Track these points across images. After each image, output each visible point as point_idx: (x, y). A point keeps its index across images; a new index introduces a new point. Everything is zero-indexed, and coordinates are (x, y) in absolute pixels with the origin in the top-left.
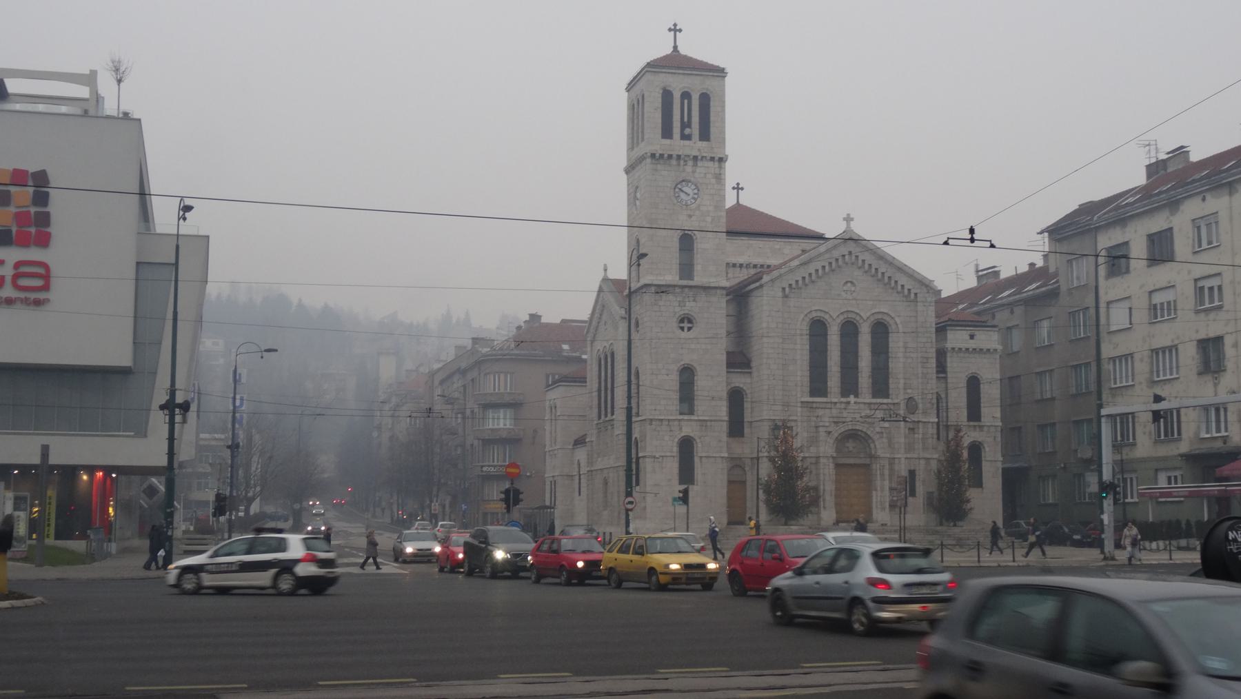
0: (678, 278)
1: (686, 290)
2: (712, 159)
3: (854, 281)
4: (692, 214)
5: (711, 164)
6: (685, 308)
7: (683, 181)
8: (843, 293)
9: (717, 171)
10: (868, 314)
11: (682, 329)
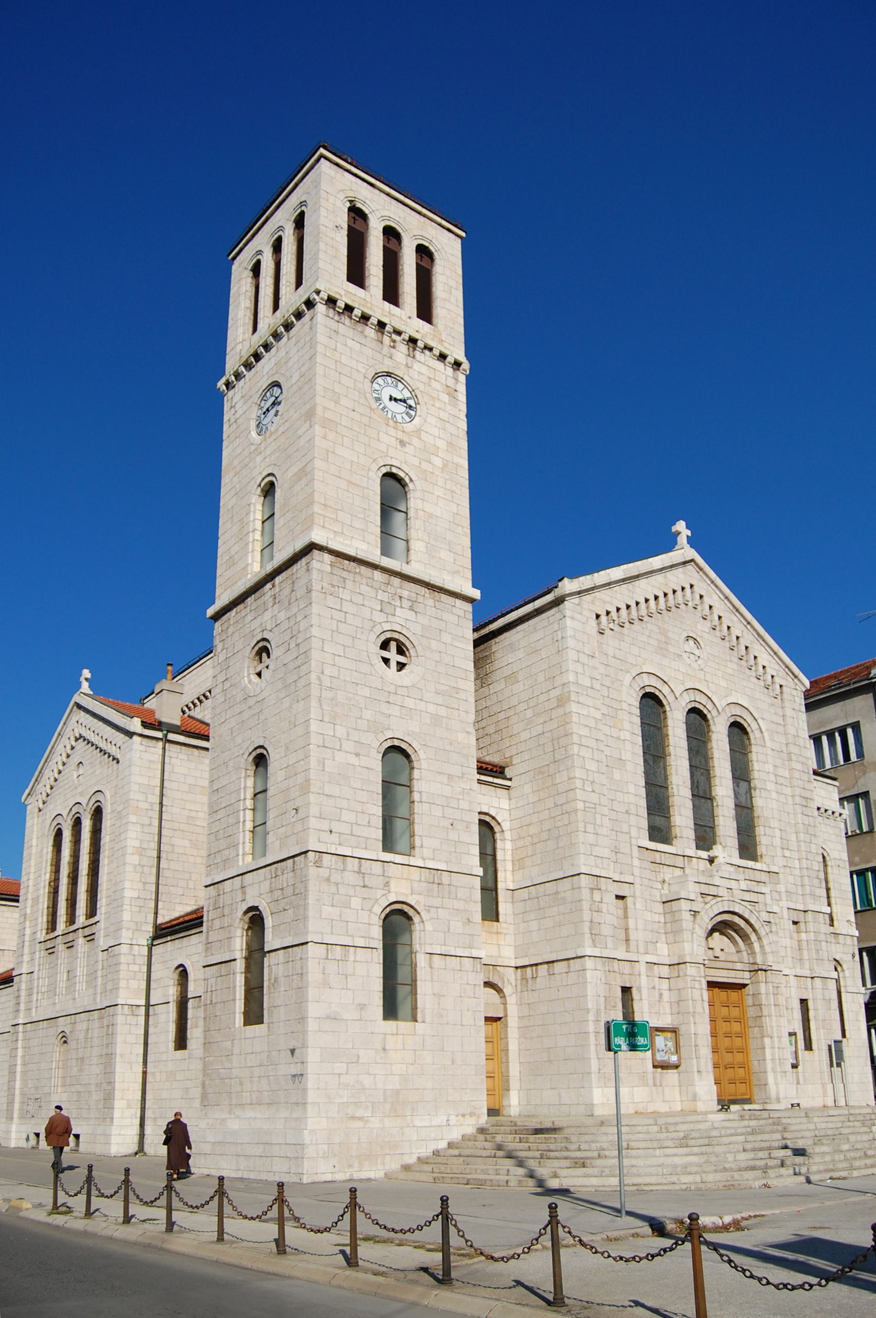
0: (378, 551)
1: (396, 581)
2: (443, 357)
3: (698, 639)
4: (406, 439)
5: (439, 365)
6: (391, 618)
7: (389, 374)
8: (685, 655)
9: (451, 382)
10: (724, 703)
11: (386, 661)
